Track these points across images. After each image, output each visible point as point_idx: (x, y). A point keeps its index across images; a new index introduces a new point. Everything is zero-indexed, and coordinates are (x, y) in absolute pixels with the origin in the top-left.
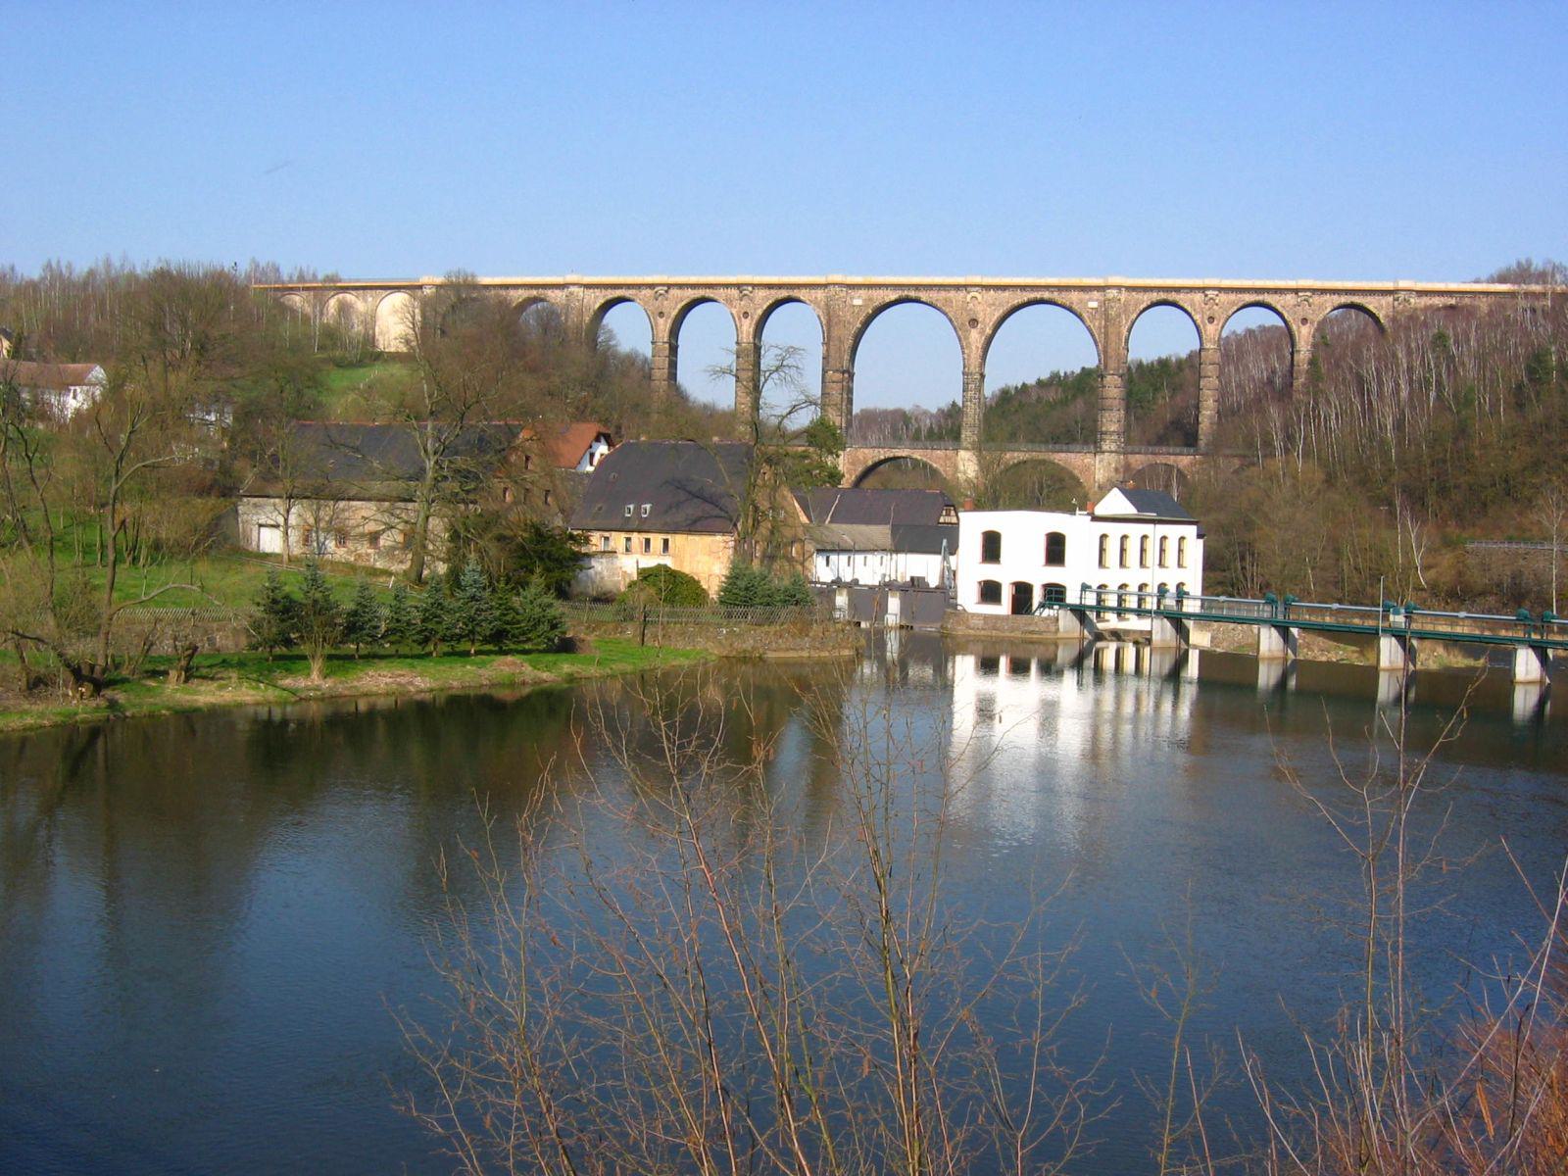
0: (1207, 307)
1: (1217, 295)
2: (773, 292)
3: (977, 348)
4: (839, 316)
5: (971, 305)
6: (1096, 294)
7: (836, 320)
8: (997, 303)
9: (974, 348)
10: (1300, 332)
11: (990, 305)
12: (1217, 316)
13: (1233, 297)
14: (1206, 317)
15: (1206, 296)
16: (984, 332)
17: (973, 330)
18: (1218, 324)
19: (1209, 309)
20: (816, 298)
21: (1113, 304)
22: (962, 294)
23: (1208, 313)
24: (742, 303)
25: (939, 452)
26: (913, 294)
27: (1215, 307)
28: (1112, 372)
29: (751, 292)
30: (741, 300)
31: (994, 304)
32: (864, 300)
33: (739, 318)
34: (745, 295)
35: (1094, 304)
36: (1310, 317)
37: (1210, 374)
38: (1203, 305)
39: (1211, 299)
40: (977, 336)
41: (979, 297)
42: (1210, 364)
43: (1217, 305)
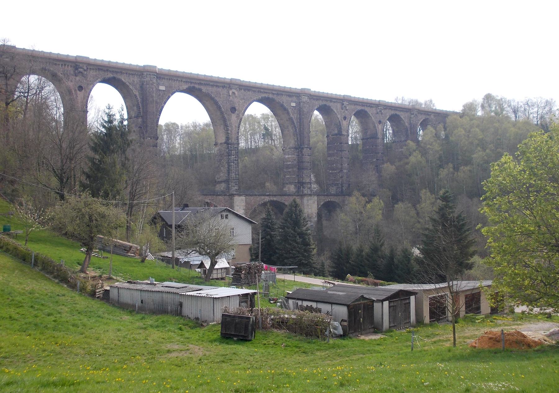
0: (343, 111)
1: (348, 105)
2: (101, 72)
3: (236, 126)
4: (152, 97)
5: (231, 98)
6: (294, 99)
7: (151, 99)
8: (245, 97)
9: (234, 127)
10: (378, 128)
11: (241, 99)
12: (347, 116)
13: (353, 107)
14: (343, 117)
15: (343, 104)
16: (239, 116)
17: (233, 114)
18: (347, 121)
19: (344, 112)
20: (134, 81)
21: (305, 105)
22: (225, 91)
23: (343, 114)
24: (78, 78)
25: (220, 197)
26: (197, 86)
27: (346, 112)
28: (306, 146)
29: (85, 70)
30: (76, 76)
31: (244, 99)
32: (166, 87)
33: (75, 90)
34: (82, 73)
35: (293, 104)
36: (382, 120)
37: (345, 149)
38: (341, 110)
39: (345, 107)
40: (235, 119)
41: (236, 93)
42: (345, 144)
43: (347, 110)
